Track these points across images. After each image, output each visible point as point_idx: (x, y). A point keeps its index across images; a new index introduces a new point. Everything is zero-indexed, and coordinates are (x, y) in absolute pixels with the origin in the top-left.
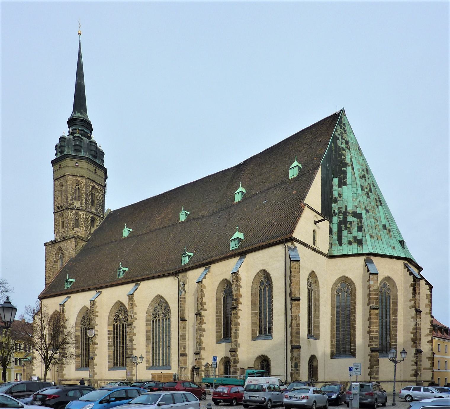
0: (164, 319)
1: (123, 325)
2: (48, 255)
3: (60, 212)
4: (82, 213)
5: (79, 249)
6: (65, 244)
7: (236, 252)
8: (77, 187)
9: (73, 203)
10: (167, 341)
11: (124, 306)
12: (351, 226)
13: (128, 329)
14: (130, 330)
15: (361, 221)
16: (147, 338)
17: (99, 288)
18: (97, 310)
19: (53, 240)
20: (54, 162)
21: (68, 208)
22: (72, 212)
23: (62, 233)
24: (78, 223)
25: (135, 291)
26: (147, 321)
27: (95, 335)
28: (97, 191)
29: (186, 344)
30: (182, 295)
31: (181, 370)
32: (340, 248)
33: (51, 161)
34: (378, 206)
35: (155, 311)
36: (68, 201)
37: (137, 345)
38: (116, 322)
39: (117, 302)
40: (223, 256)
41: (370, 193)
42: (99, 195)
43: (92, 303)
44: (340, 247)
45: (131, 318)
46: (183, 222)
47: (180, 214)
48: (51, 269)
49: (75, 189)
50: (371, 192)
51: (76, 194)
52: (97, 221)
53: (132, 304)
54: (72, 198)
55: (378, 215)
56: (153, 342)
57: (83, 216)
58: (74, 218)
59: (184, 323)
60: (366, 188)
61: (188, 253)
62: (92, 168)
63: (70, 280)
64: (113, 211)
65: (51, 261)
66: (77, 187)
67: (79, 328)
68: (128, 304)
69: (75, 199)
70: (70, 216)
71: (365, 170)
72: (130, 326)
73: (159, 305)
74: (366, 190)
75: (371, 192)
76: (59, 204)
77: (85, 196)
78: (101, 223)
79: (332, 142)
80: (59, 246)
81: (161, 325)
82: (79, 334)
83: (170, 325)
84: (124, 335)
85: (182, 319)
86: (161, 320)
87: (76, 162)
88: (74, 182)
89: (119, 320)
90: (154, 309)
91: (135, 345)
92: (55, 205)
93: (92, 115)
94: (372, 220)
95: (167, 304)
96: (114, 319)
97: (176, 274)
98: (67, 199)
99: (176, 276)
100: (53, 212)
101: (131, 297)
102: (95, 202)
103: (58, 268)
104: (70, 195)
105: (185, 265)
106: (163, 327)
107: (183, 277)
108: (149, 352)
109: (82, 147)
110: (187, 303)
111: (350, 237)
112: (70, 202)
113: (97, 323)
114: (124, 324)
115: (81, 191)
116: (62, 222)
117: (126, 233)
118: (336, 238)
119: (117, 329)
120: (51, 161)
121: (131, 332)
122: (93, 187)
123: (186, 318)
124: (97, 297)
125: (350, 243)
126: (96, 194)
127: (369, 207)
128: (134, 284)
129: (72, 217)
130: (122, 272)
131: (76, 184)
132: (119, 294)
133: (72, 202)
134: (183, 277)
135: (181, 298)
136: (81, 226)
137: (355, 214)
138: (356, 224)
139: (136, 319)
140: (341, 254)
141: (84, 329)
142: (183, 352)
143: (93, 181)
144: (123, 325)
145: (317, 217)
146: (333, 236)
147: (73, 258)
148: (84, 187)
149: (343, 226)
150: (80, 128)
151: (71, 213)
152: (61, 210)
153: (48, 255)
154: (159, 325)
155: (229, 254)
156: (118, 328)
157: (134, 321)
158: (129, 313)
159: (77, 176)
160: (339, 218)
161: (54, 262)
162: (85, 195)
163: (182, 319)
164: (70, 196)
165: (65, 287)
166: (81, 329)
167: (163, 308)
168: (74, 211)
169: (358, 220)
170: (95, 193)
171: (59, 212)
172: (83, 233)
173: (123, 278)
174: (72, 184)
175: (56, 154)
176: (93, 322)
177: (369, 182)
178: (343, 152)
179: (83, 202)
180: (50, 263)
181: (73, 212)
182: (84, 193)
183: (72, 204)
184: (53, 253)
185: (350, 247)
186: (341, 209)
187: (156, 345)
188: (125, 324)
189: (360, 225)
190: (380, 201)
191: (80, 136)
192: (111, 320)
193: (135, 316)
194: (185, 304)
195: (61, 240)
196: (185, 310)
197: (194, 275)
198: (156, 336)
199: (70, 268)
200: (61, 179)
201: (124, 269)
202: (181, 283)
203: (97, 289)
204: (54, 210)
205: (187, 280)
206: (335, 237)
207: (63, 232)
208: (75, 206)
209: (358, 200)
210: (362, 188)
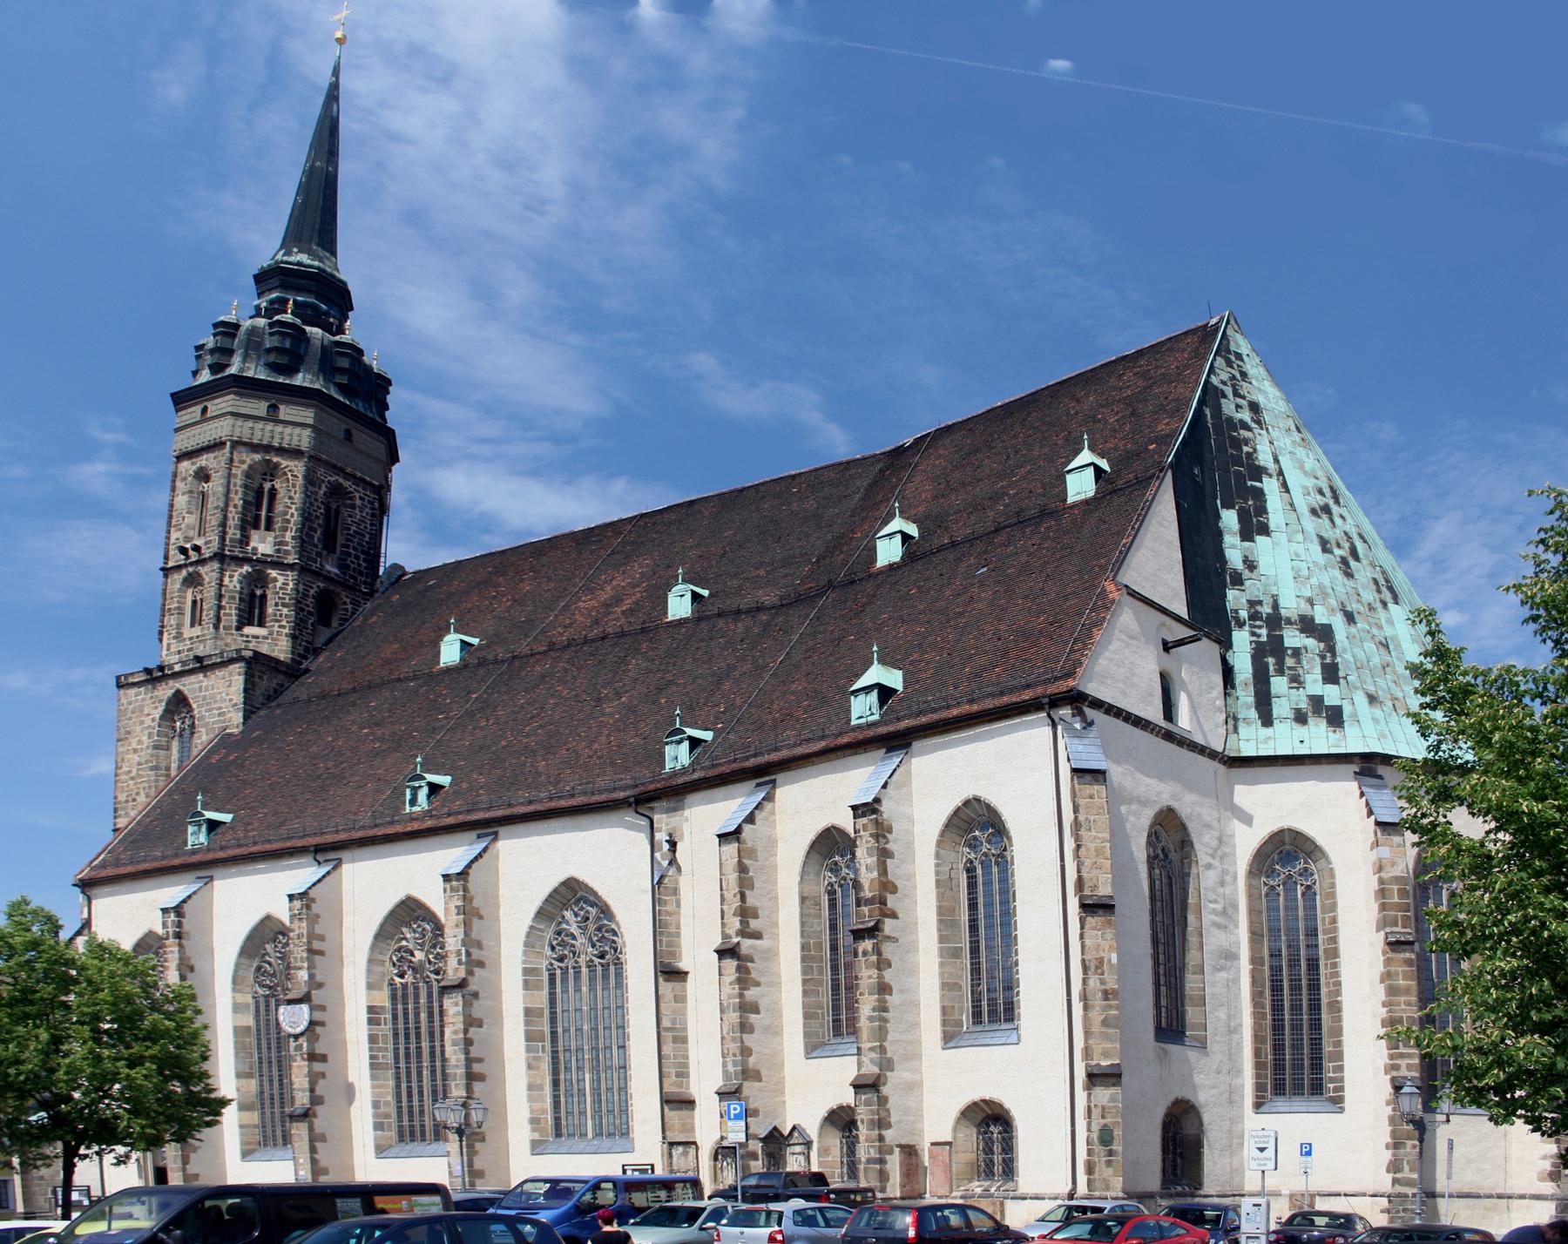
3: (191, 569)
7: (871, 733)
12: (1299, 662)
15: (1331, 649)
16: (530, 1037)
17: (328, 850)
26: (526, 971)
31: (670, 1155)
32: (1266, 732)
34: (1384, 604)
38: (402, 976)
40: (822, 744)
41: (1352, 563)
44: (1268, 731)
50: (1357, 559)
55: (1388, 631)
56: (555, 1053)
60: (1339, 546)
61: (690, 732)
71: (1327, 491)
74: (1337, 552)
75: (1357, 559)
76: (188, 539)
79: (1201, 402)
85: (669, 972)
86: (584, 970)
91: (480, 1060)
94: (1370, 646)
101: (458, 879)
105: (675, 774)
108: (540, 1088)
110: (685, 910)
111: (1301, 699)
118: (1251, 700)
119: (405, 1003)
125: (1300, 718)
127: (1353, 606)
130: (425, 790)
135: (662, 887)
137: (1307, 625)
138: (1318, 659)
140: (1271, 753)
142: (674, 1089)
144: (430, 987)
145: (1169, 629)
146: (1240, 692)
147: (231, 735)
149: (1271, 660)
152: (193, 559)
155: (845, 740)
160: (1253, 634)
163: (669, 972)
167: (592, 927)
168: (247, 568)
169: (1322, 645)
171: (185, 566)
173: (428, 814)
177: (1347, 528)
178: (1244, 433)
185: (1301, 732)
186: (1259, 608)
189: (1328, 661)
190: (1391, 589)
192: (379, 969)
196: (678, 935)
197: (706, 818)
199: (215, 774)
201: (430, 778)
202: (661, 837)
204: (166, 558)
205: (686, 828)
206: (1245, 695)
209: (1314, 581)
210: (1325, 545)
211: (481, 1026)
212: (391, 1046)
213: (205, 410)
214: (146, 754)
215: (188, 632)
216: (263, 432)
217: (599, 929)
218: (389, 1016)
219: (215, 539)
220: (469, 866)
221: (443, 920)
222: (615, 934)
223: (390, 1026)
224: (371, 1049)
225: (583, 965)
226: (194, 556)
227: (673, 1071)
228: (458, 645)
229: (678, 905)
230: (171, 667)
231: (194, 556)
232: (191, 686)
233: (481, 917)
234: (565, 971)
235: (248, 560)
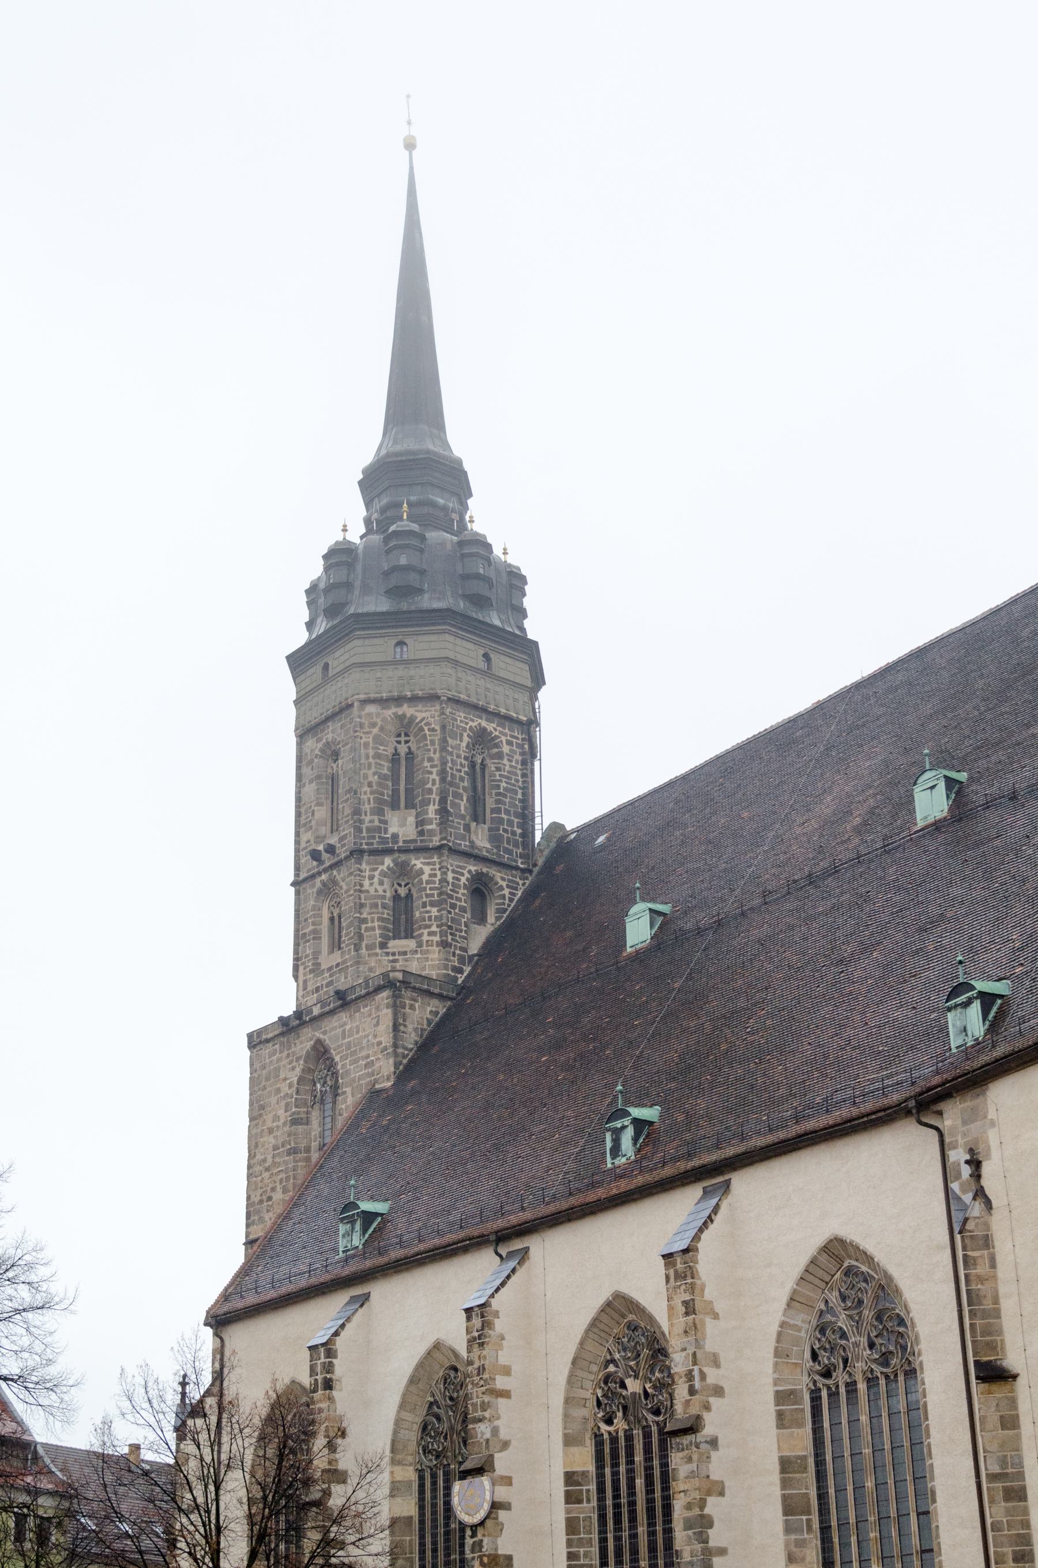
0: (882, 1382)
1: (647, 1435)
2: (264, 1088)
3: (324, 877)
4: (428, 864)
5: (411, 1038)
6: (345, 1024)
8: (403, 749)
9: (385, 822)
10: (913, 1517)
11: (651, 1319)
13: (676, 1459)
14: (690, 1460)
16: (790, 1507)
17: (509, 1236)
18: (503, 1359)
19: (288, 1009)
20: (298, 662)
21: (361, 852)
22: (381, 867)
23: (331, 976)
24: (409, 912)
25: (701, 1230)
26: (781, 1397)
27: (495, 1506)
28: (496, 750)
29: (1026, 1524)
30: (970, 1226)
33: (288, 658)
35: (822, 1330)
36: (363, 817)
37: (730, 1551)
38: (609, 1421)
39: (609, 1304)
42: (507, 768)
43: (477, 1322)
45: (692, 1391)
46: (937, 826)
47: (917, 789)
48: (277, 1160)
49: (395, 758)
51: (396, 781)
52: (501, 888)
53: (689, 1308)
54: (380, 801)
56: (825, 1529)
57: (430, 876)
58: (388, 894)
59: (999, 1391)
62: (469, 651)
63: (366, 1206)
64: (579, 830)
65: (276, 1118)
66: (403, 749)
67: (410, 1474)
68: (671, 1308)
69: (395, 805)
70: (371, 884)
72: (686, 1440)
73: (844, 1298)
76: (319, 839)
77: (437, 782)
78: (516, 899)
80: (319, 1042)
81: (864, 1419)
82: (408, 1507)
83: (916, 1412)
84: (658, 1494)
86: (862, 1386)
87: (395, 641)
88: (389, 727)
89: (625, 1408)
90: (814, 1322)
92: (303, 845)
93: (464, 436)
95: (885, 1289)
96: (599, 1404)
97: (924, 1104)
98: (357, 812)
99: (924, 1120)
100: (292, 878)
101: (680, 1263)
102: (490, 803)
103: (308, 1150)
104: (368, 789)
106: (876, 1432)
107: (965, 1123)
109: (422, 572)
110: (1004, 1271)
112: (369, 820)
113: (503, 1435)
114: (654, 1429)
115: (423, 759)
116: (332, 919)
117: (638, 930)
119: (615, 1465)
120: (288, 658)
121: (691, 1475)
122: (481, 738)
123: (1012, 1360)
124: (503, 1284)
126: (491, 767)
128: (693, 1193)
129: (380, 889)
130: (630, 1132)
131: (399, 735)
132: (617, 1256)
133: (380, 821)
134: (965, 1123)
136: (420, 928)
139: (719, 1391)
141: (434, 1476)
143: (475, 707)
148: (433, 743)
150: (413, 498)
152: (327, 864)
153: (264, 1088)
154: (853, 1422)
156: (622, 1453)
157: (707, 1407)
158: (679, 1362)
159: (399, 700)
161: (295, 1122)
162: (437, 779)
164: (372, 793)
165: (341, 1249)
166: (421, 1478)
167: (868, 1314)
168: (388, 861)
170: (488, 761)
171: (319, 874)
172: (430, 956)
174: (377, 740)
175: (310, 625)
176: (482, 1431)
179: (432, 810)
180: (271, 1131)
181: (384, 867)
182: (434, 770)
183: (378, 829)
184: (285, 1079)
187: (845, 1545)
188: (661, 1432)
191: (415, 527)
192: (580, 1413)
193: (713, 1376)
194: (995, 1277)
195: (327, 1009)
196: (997, 1313)
198: (840, 1490)
200: (330, 724)
201: (636, 1112)
202: (958, 1156)
203: (502, 1237)
207: (338, 965)
208: (395, 836)
211: (722, 1494)
212: (595, 1537)
213: (326, 667)
214: (281, 1135)
215: (327, 960)
216: (389, 682)
217: (879, 1317)
218: (593, 1487)
219: (347, 830)
220: (697, 1238)
221: (665, 1328)
222: (902, 1322)
223: (594, 1503)
224: (569, 1544)
225: (859, 1377)
226: (328, 860)
227: (1008, 1550)
228: (646, 918)
229: (993, 1265)
230: (309, 1011)
231: (328, 860)
232: (336, 1032)
233: (716, 1316)
234: (833, 1395)
235: (389, 852)
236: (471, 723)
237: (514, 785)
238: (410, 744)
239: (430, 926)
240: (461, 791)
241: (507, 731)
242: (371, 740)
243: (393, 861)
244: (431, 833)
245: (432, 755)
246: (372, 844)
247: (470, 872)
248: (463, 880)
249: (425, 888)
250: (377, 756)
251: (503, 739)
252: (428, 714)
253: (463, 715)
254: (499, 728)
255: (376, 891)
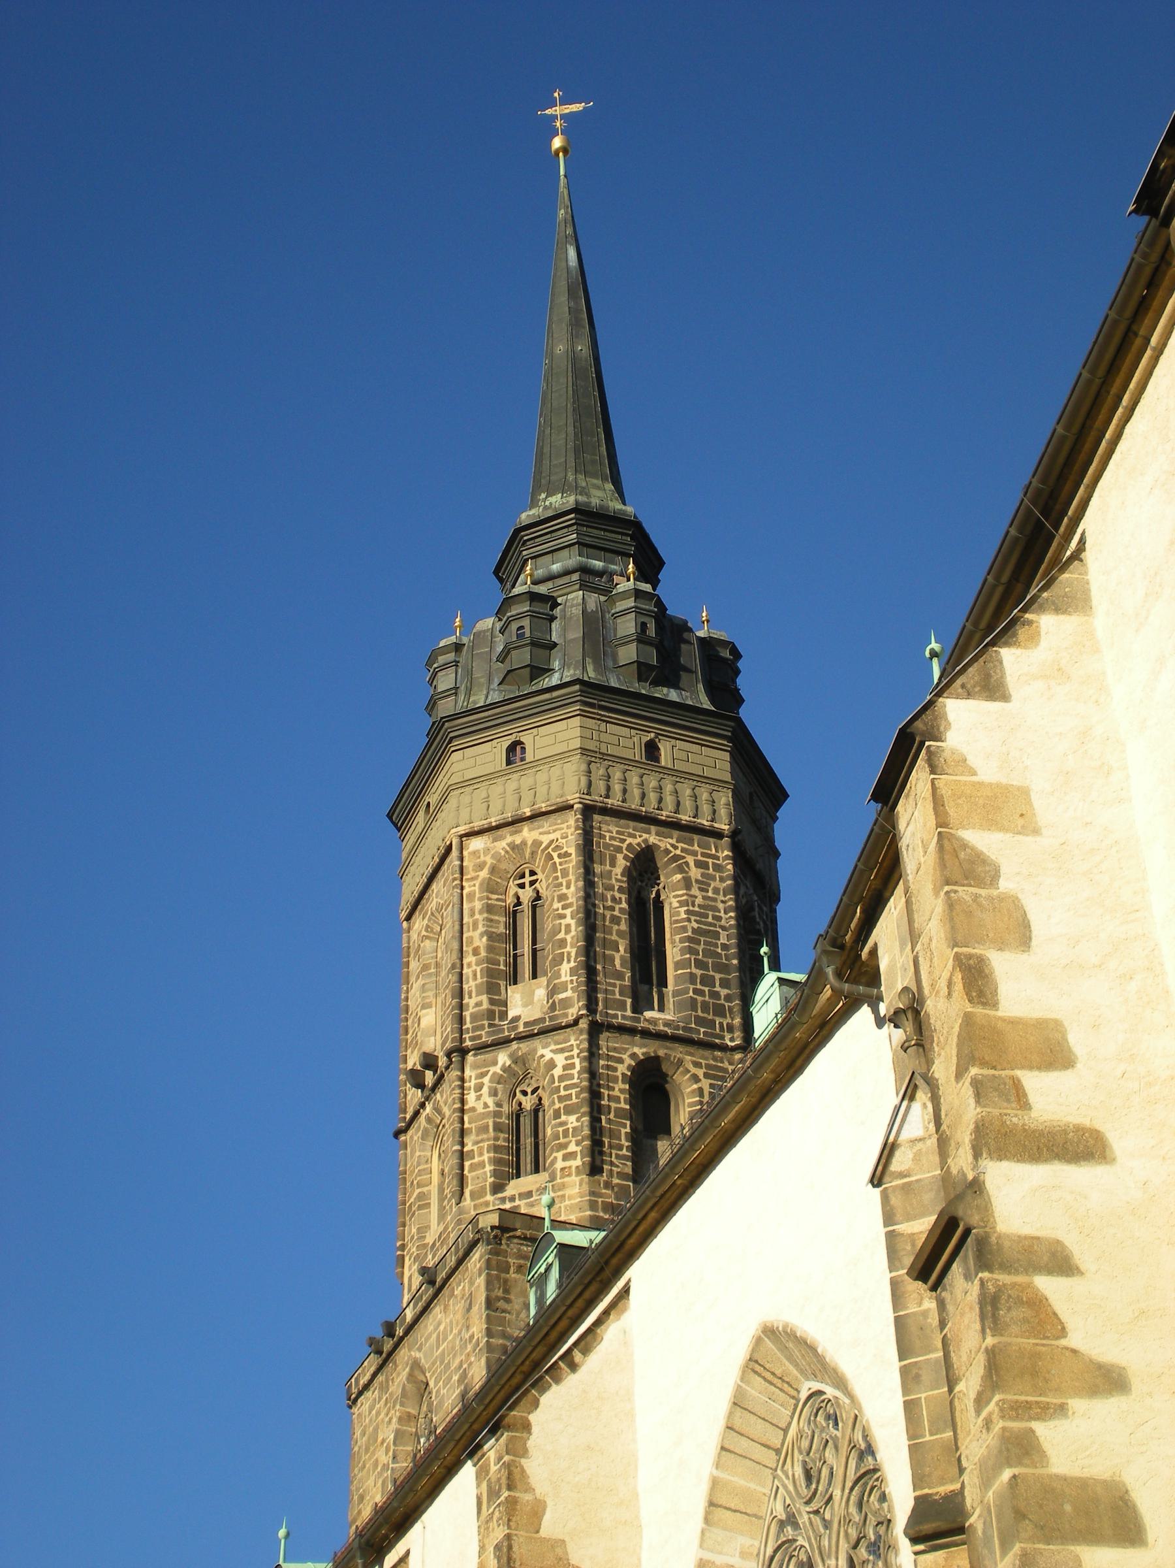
4: (562, 1050)
8: (526, 895)
22: (493, 1069)
54: (490, 973)
57: (565, 1068)
70: (479, 1098)
77: (573, 928)
112: (476, 1002)
151: (483, 1075)
164: (477, 965)
168: (504, 1057)
172: (568, 1192)
181: (497, 1069)
182: (568, 912)
236: (629, 840)
237: (710, 924)
238: (537, 885)
239: (565, 1146)
240: (614, 937)
241: (696, 847)
242: (477, 888)
243: (511, 1056)
244: (566, 1003)
245: (564, 891)
246: (480, 1037)
247: (633, 1056)
248: (622, 1069)
249: (558, 1089)
250: (489, 909)
251: (690, 860)
252: (557, 835)
253: (615, 829)
254: (680, 845)
255: (486, 1105)
